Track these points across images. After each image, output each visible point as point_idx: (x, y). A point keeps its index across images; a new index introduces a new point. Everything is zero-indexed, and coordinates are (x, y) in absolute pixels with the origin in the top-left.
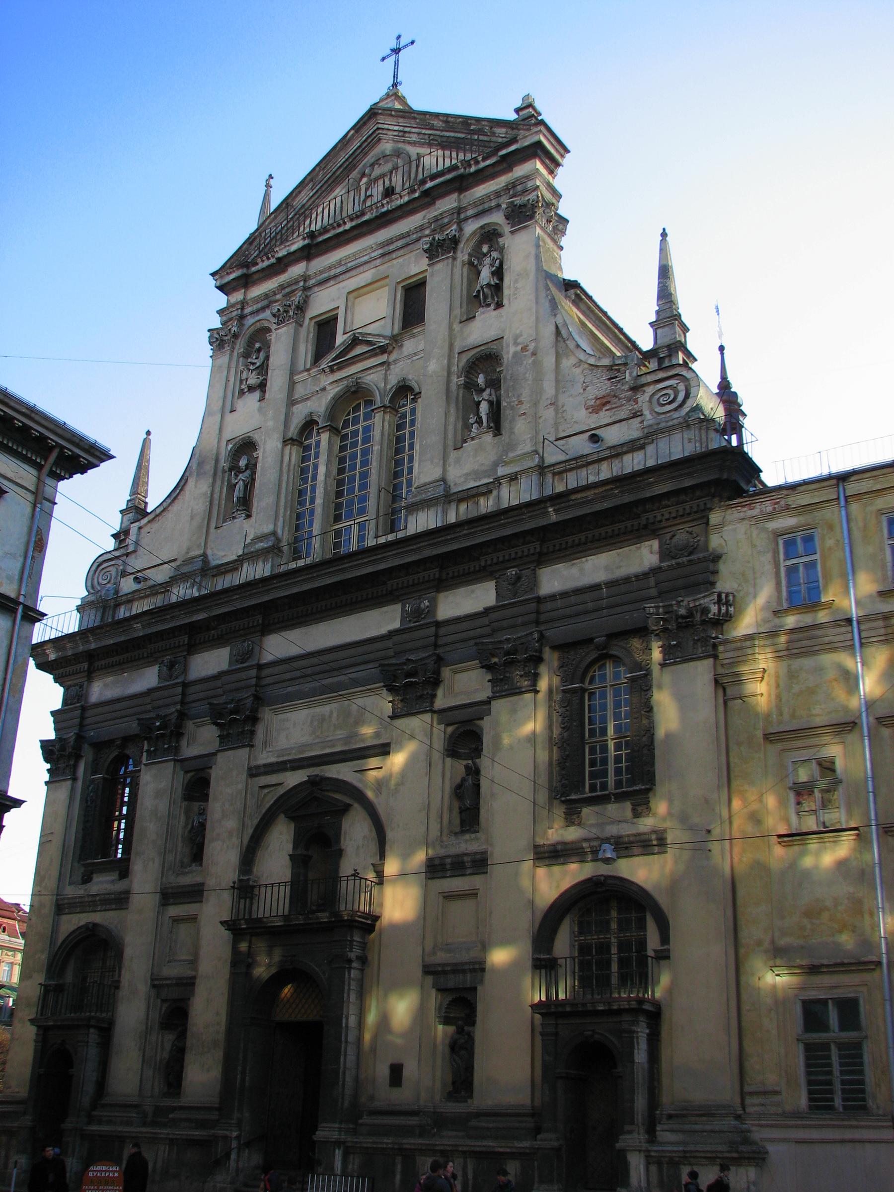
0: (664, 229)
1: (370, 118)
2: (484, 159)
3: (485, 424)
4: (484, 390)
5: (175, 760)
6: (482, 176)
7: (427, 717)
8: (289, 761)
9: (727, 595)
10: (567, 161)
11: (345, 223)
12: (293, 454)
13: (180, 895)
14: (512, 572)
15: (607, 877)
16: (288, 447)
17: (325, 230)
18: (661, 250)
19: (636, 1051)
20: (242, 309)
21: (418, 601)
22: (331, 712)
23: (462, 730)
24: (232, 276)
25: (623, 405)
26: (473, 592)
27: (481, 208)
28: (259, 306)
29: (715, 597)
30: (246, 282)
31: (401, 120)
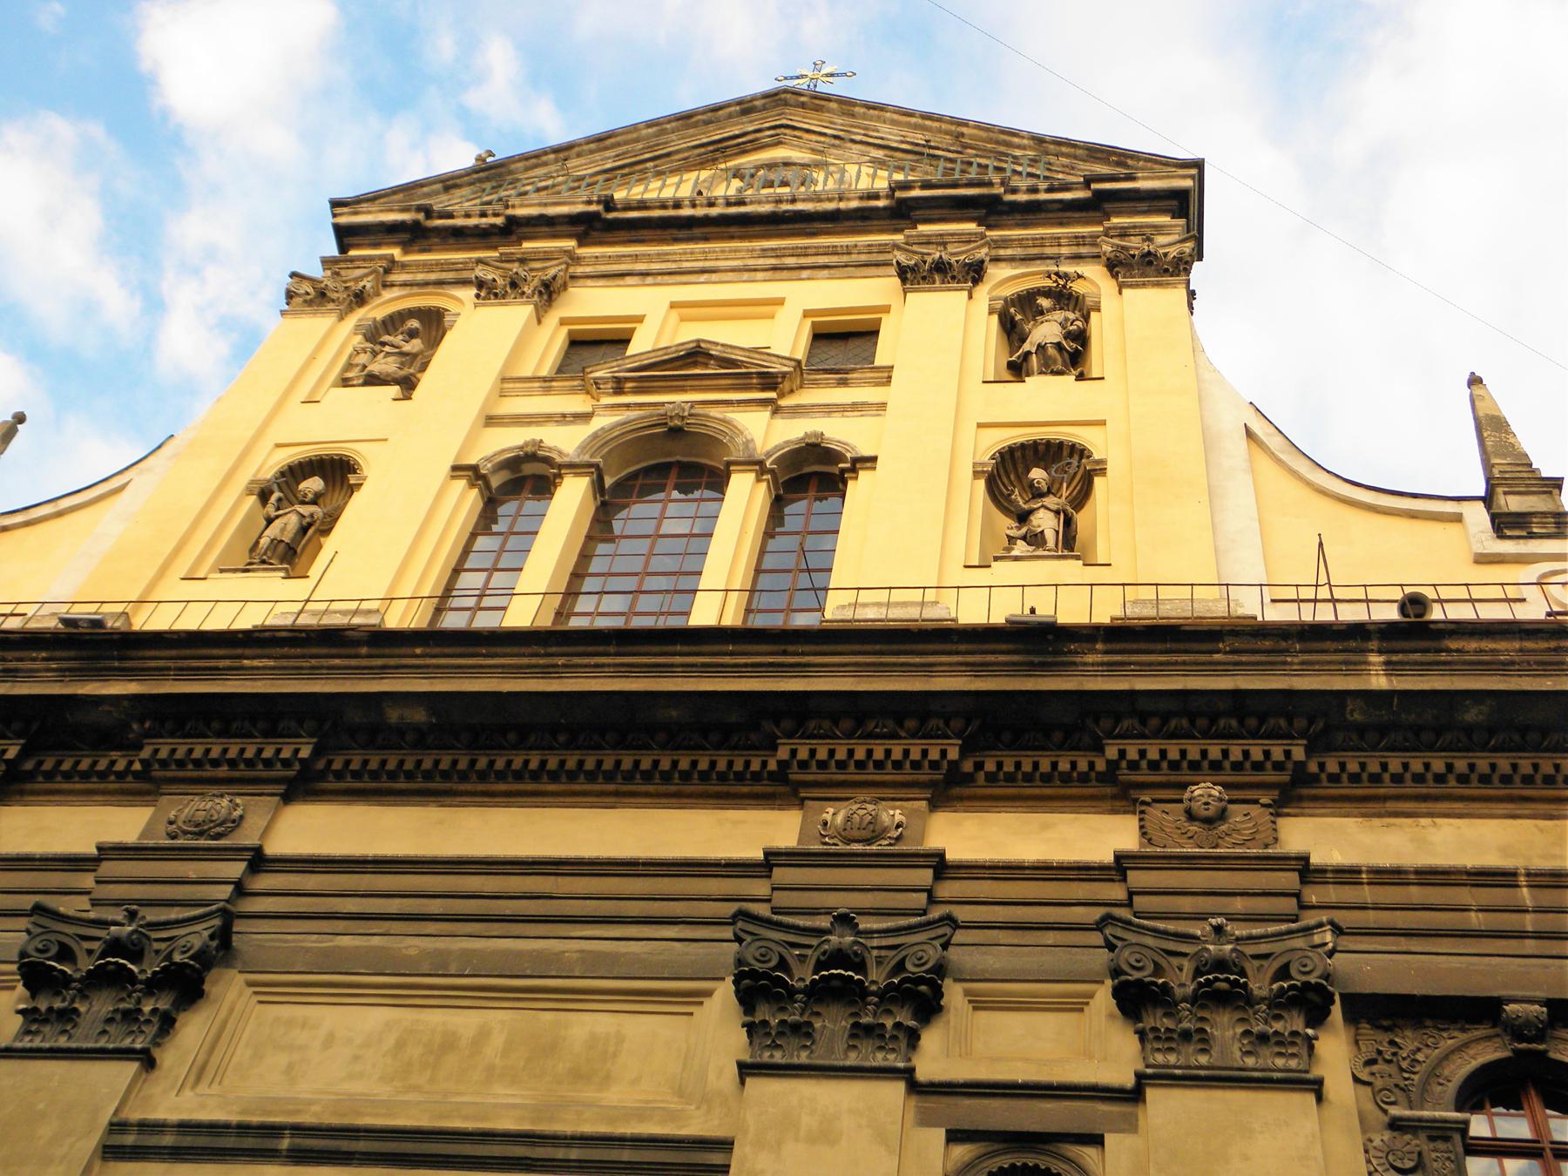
4: (1041, 495)
7: (895, 1091)
8: (298, 1129)
12: (465, 501)
14: (1205, 792)
16: (462, 483)
17: (642, 205)
21: (870, 807)
22: (483, 1034)
23: (1005, 1161)
26: (1045, 827)
28: (433, 277)
30: (413, 235)
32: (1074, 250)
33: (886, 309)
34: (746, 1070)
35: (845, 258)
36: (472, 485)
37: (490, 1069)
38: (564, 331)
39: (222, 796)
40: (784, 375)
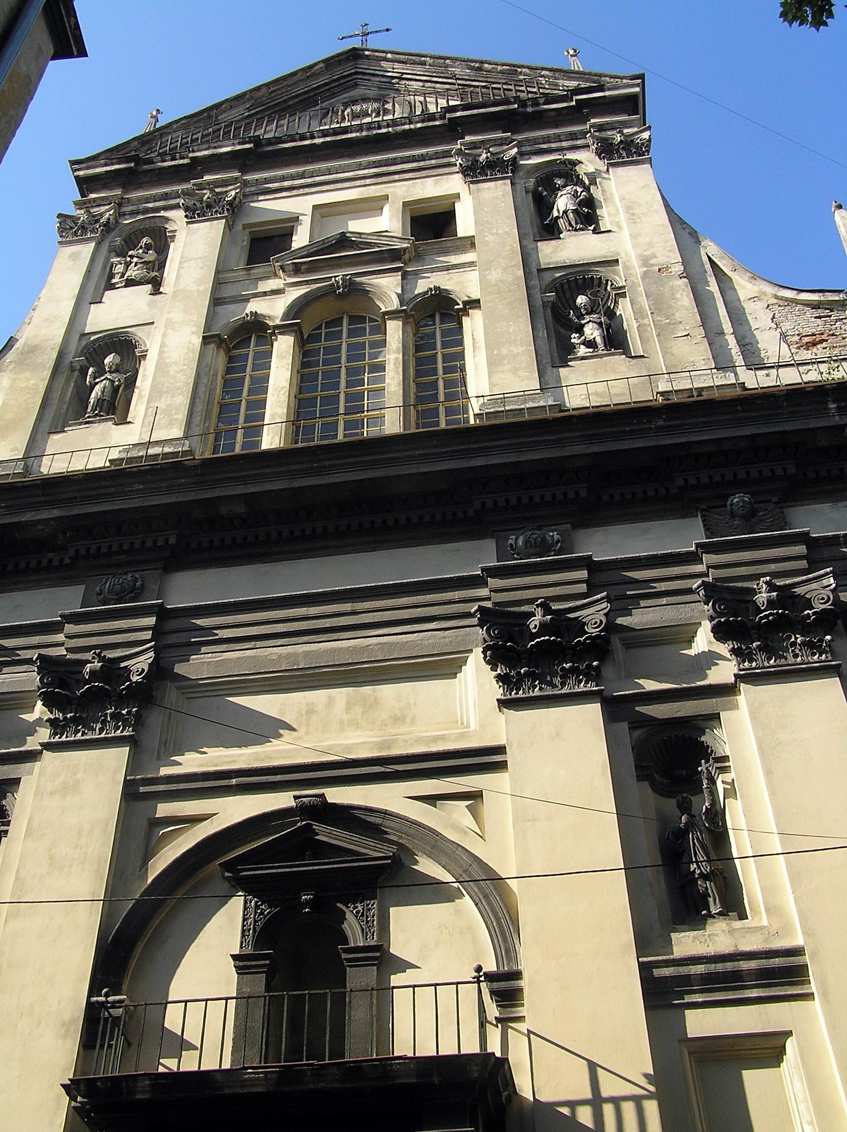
1: (347, 59)
10: (807, 30)
16: (212, 346)
20: (120, 205)
21: (539, 532)
22: (331, 702)
30: (128, 179)
32: (570, 143)
33: (457, 196)
34: (504, 704)
35: (422, 164)
37: (341, 722)
38: (247, 231)
39: (126, 574)
40: (405, 249)
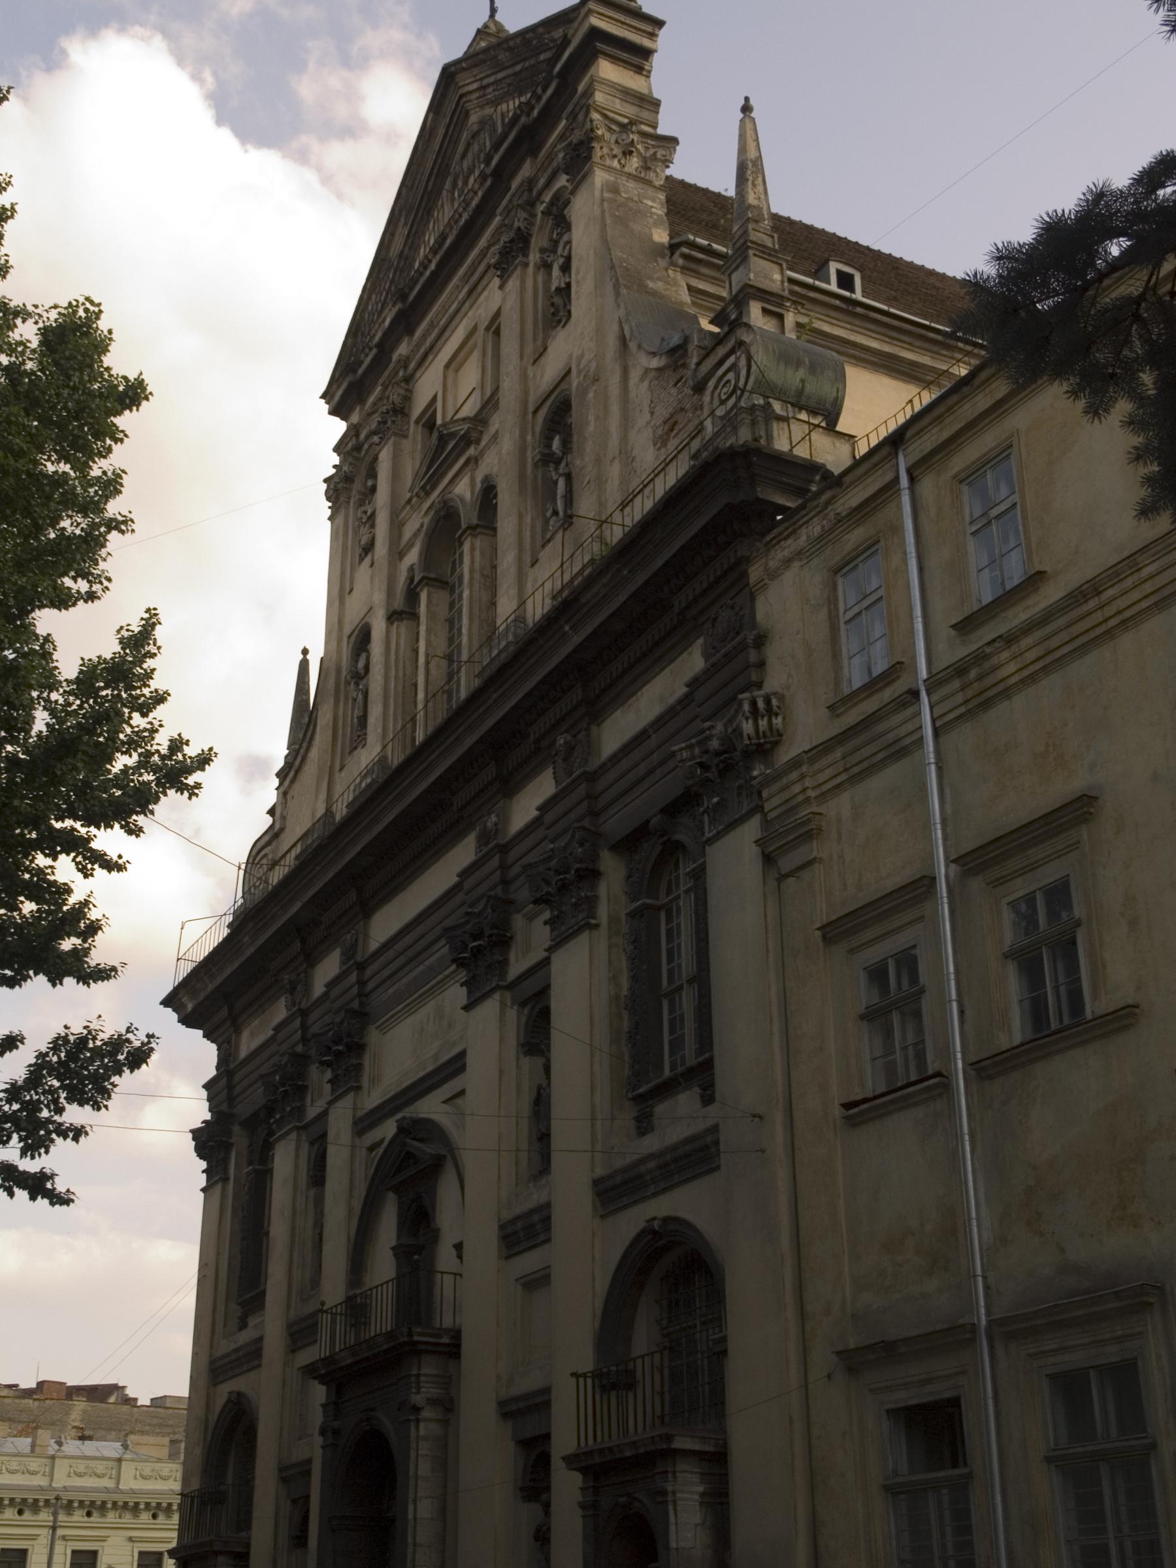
0: (747, 99)
2: (544, 91)
3: (561, 513)
4: (562, 459)
5: (298, 1128)
6: (548, 117)
9: (768, 701)
11: (430, 261)
13: (300, 1333)
15: (667, 1220)
18: (740, 140)
19: (672, 1528)
24: (340, 392)
25: (689, 421)
27: (550, 170)
29: (746, 707)
31: (475, 71)
34: (467, 1008)
36: (402, 620)
